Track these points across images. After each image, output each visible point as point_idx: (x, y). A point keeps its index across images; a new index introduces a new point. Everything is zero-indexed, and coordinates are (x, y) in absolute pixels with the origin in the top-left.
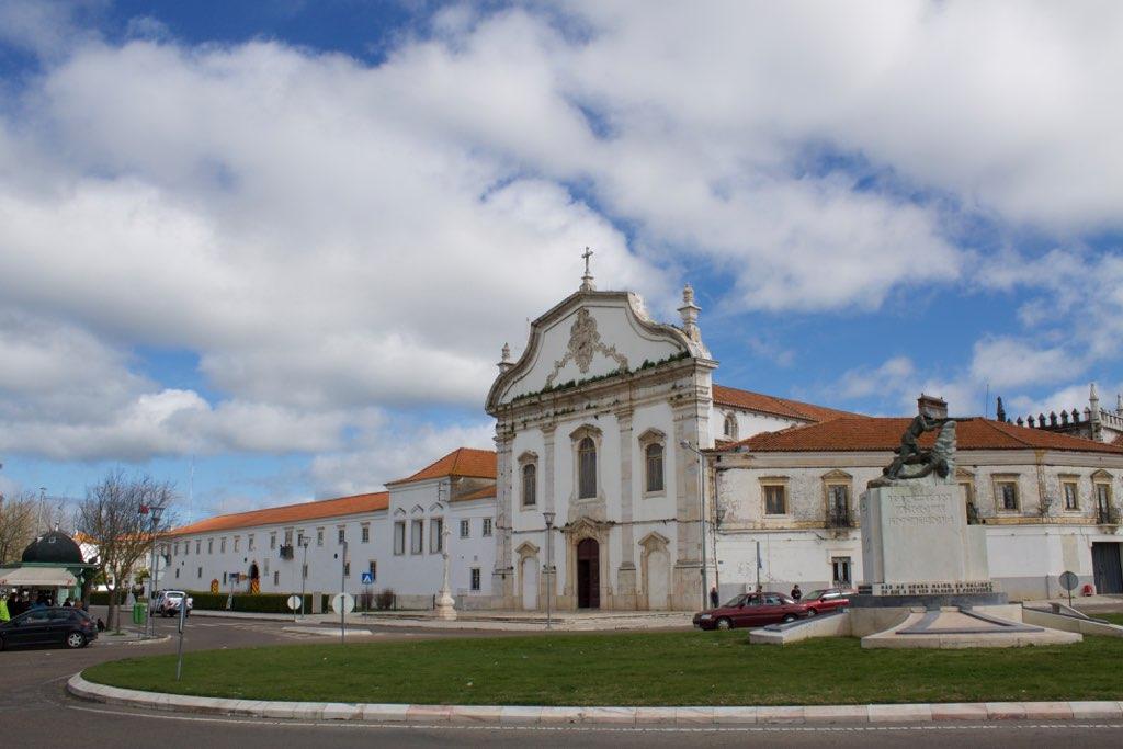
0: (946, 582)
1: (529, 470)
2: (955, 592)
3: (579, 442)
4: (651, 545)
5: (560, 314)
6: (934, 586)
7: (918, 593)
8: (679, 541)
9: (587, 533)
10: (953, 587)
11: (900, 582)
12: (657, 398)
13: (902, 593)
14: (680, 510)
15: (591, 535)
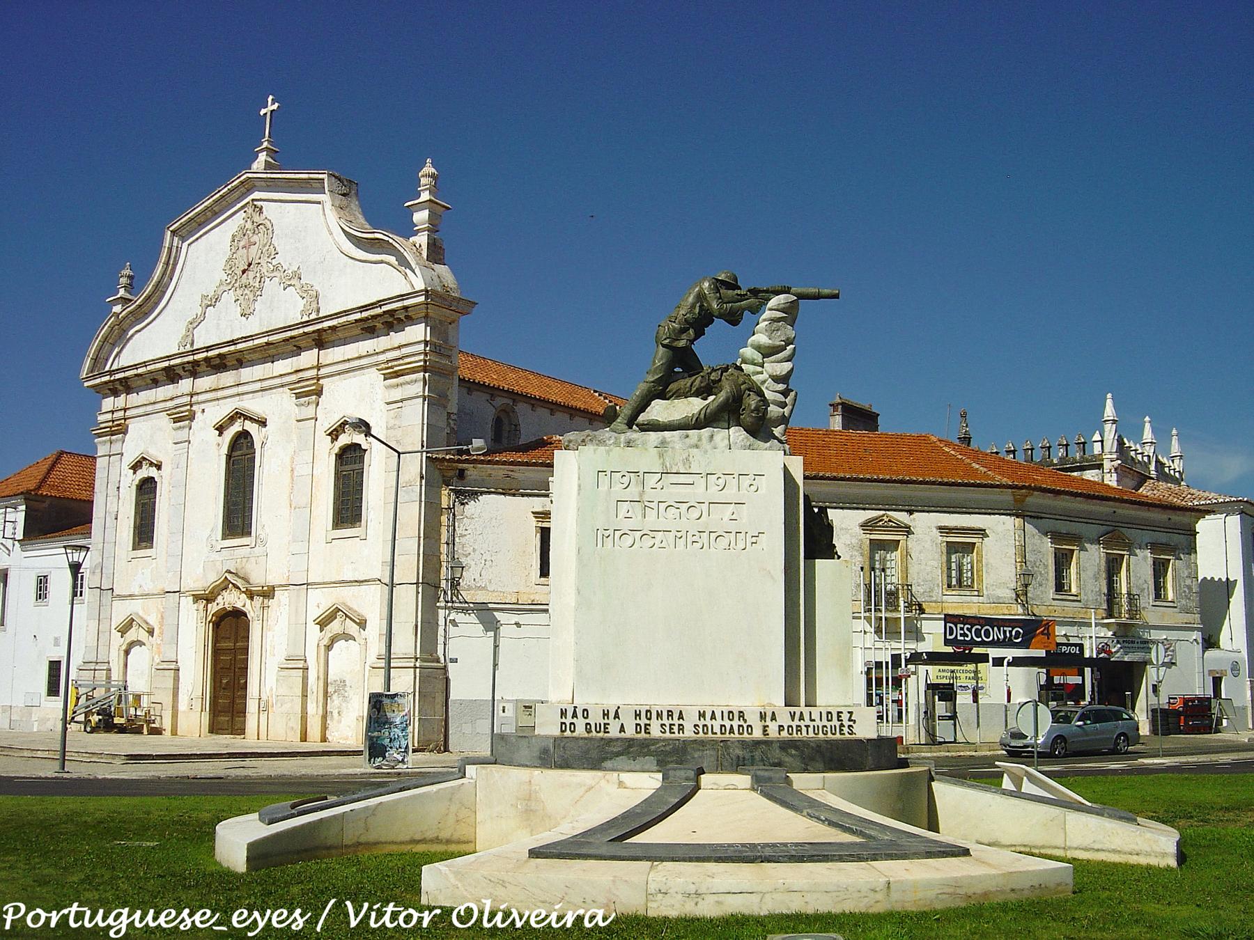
0: (736, 704)
1: (147, 488)
2: (757, 734)
4: (335, 627)
6: (702, 715)
7: (655, 732)
9: (231, 599)
10: (753, 719)
11: (611, 703)
13: (614, 732)
15: (239, 605)
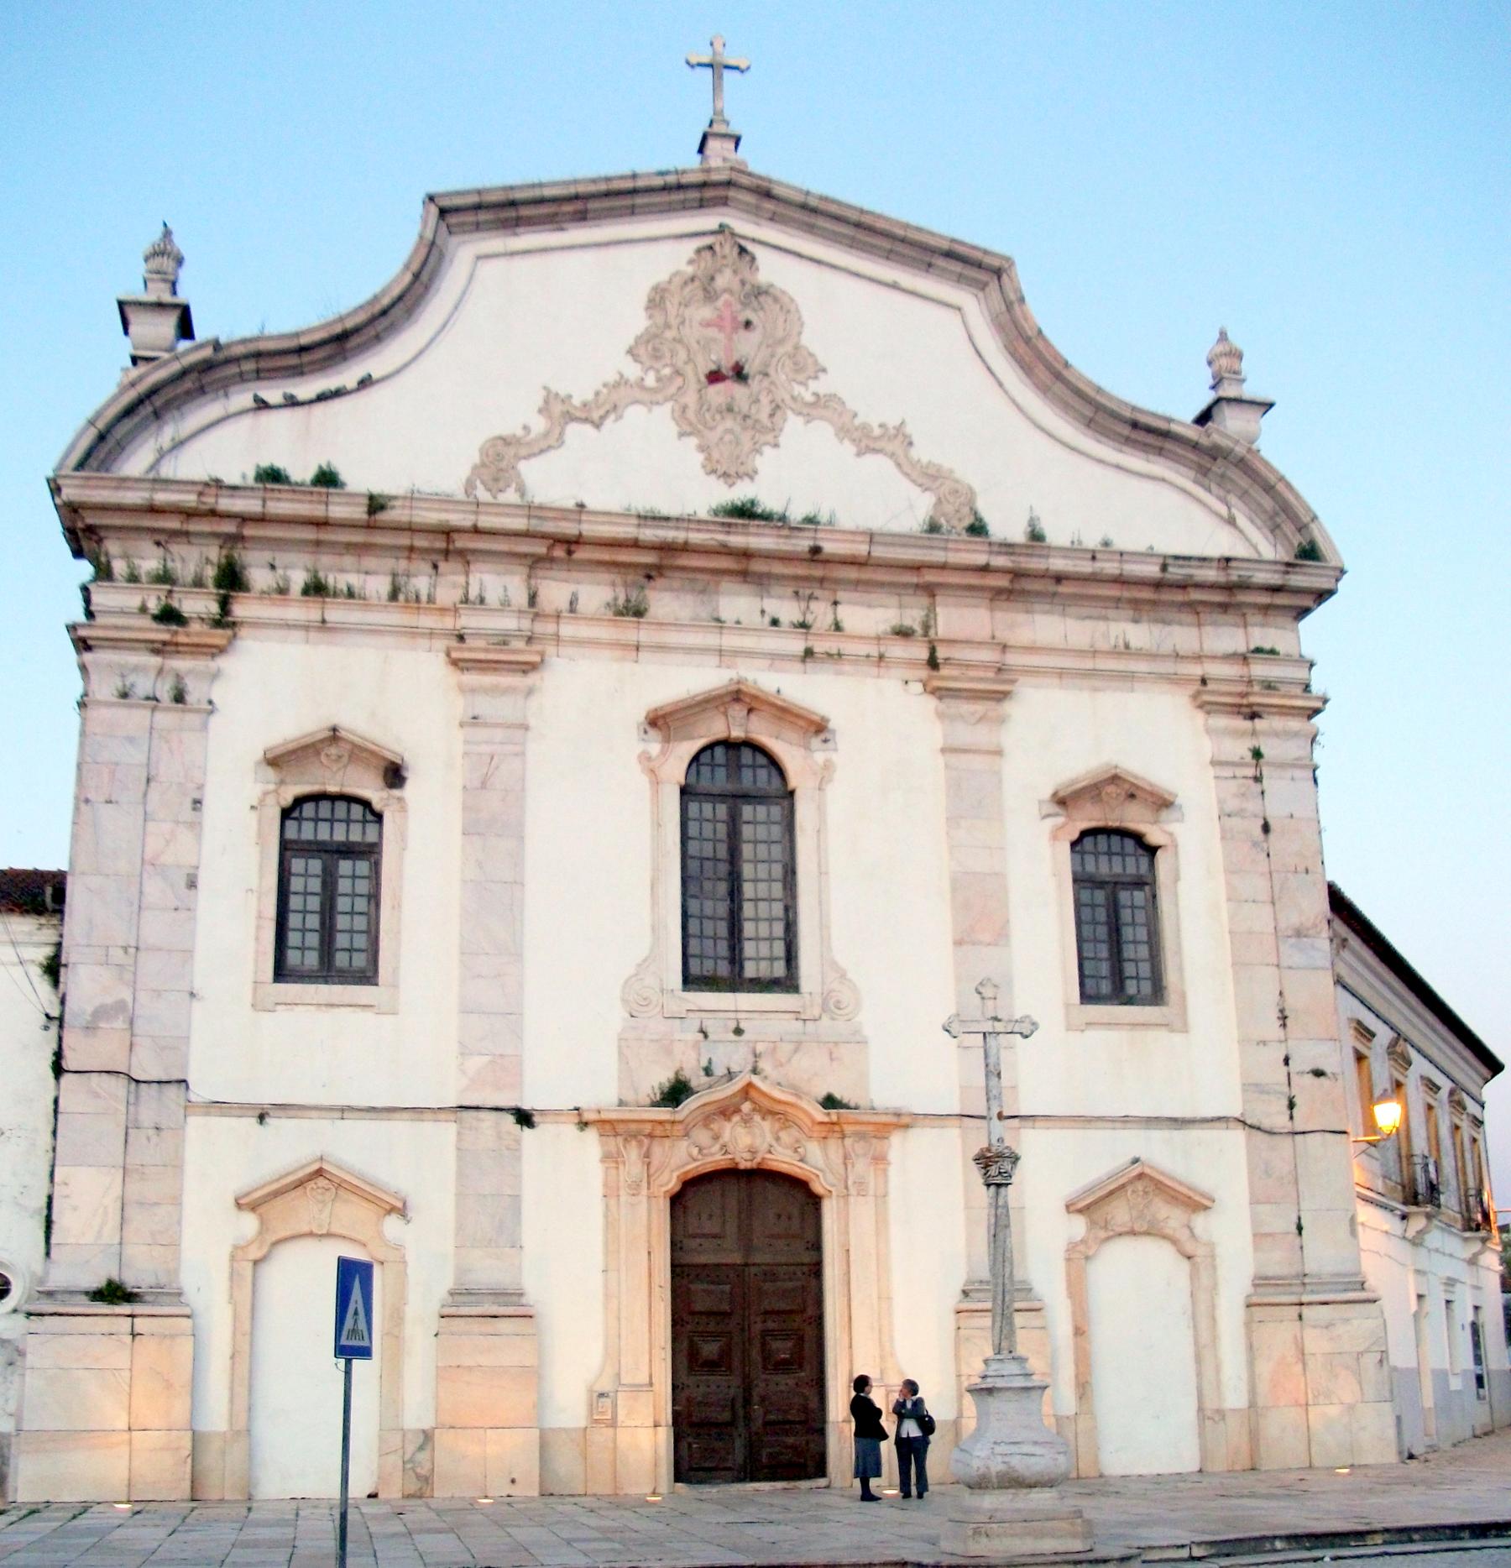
3: (690, 748)
4: (1120, 1213)
5: (582, 217)
8: (1255, 1201)
12: (1141, 666)
14: (1253, 1088)
